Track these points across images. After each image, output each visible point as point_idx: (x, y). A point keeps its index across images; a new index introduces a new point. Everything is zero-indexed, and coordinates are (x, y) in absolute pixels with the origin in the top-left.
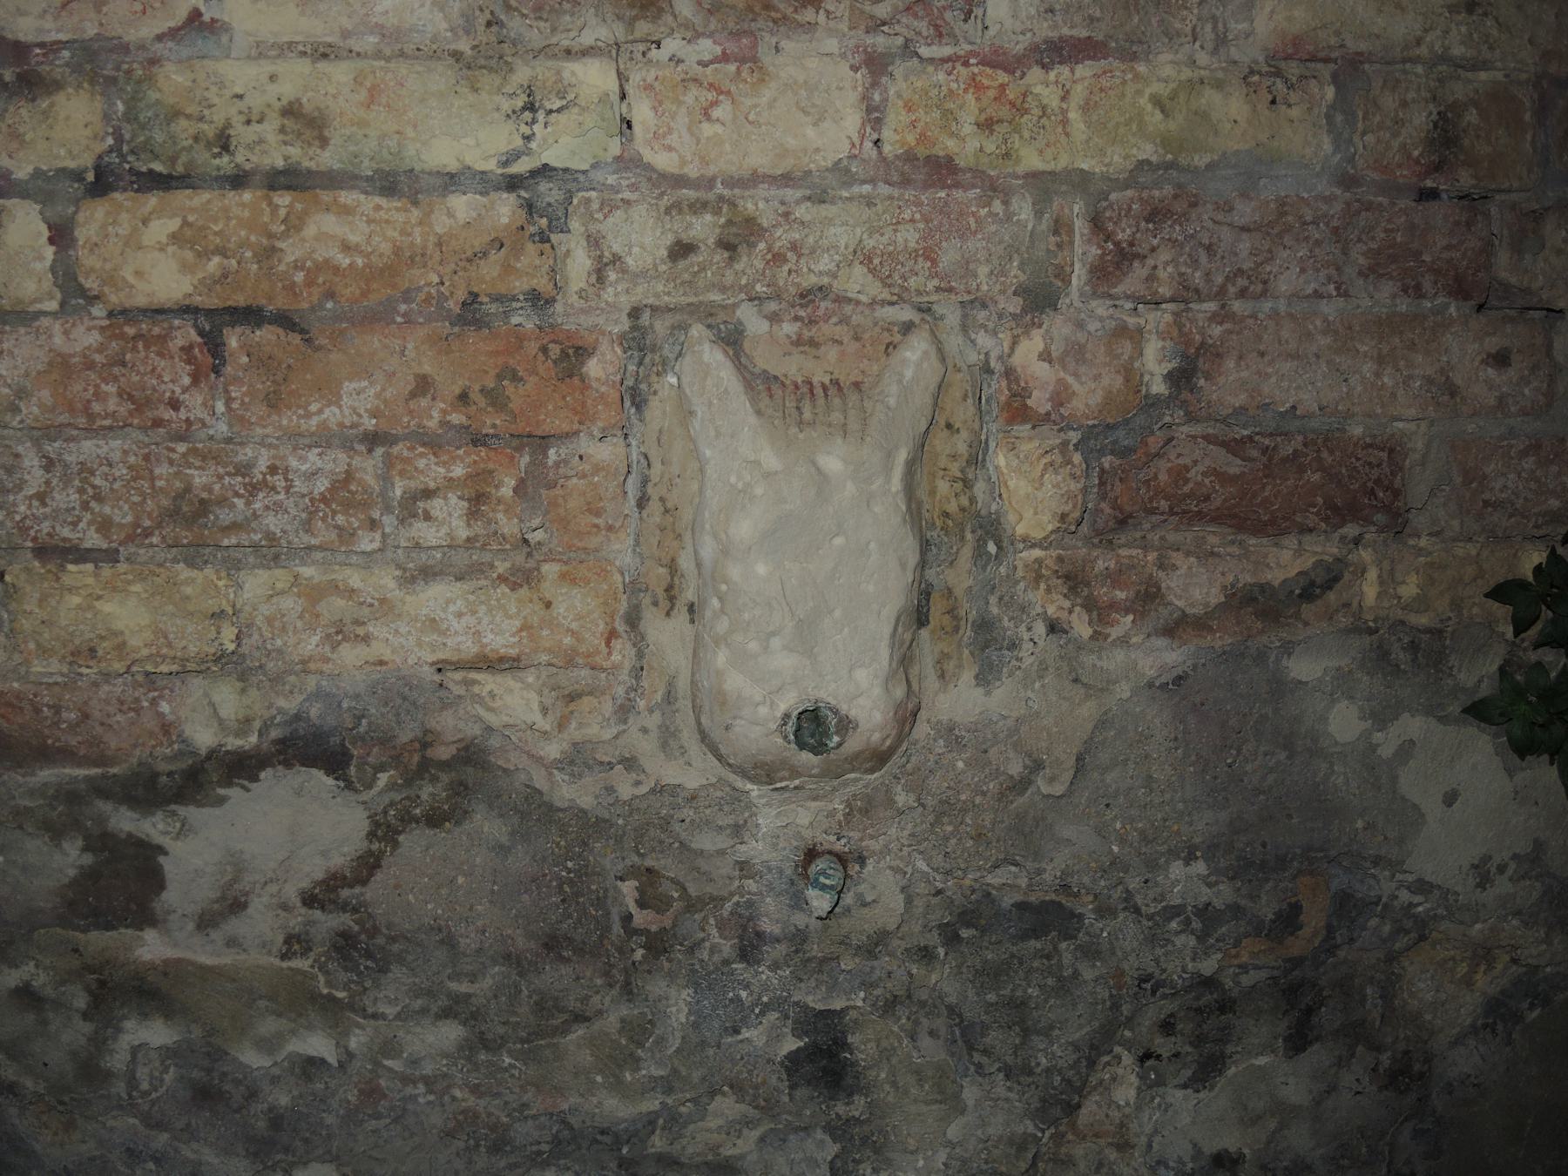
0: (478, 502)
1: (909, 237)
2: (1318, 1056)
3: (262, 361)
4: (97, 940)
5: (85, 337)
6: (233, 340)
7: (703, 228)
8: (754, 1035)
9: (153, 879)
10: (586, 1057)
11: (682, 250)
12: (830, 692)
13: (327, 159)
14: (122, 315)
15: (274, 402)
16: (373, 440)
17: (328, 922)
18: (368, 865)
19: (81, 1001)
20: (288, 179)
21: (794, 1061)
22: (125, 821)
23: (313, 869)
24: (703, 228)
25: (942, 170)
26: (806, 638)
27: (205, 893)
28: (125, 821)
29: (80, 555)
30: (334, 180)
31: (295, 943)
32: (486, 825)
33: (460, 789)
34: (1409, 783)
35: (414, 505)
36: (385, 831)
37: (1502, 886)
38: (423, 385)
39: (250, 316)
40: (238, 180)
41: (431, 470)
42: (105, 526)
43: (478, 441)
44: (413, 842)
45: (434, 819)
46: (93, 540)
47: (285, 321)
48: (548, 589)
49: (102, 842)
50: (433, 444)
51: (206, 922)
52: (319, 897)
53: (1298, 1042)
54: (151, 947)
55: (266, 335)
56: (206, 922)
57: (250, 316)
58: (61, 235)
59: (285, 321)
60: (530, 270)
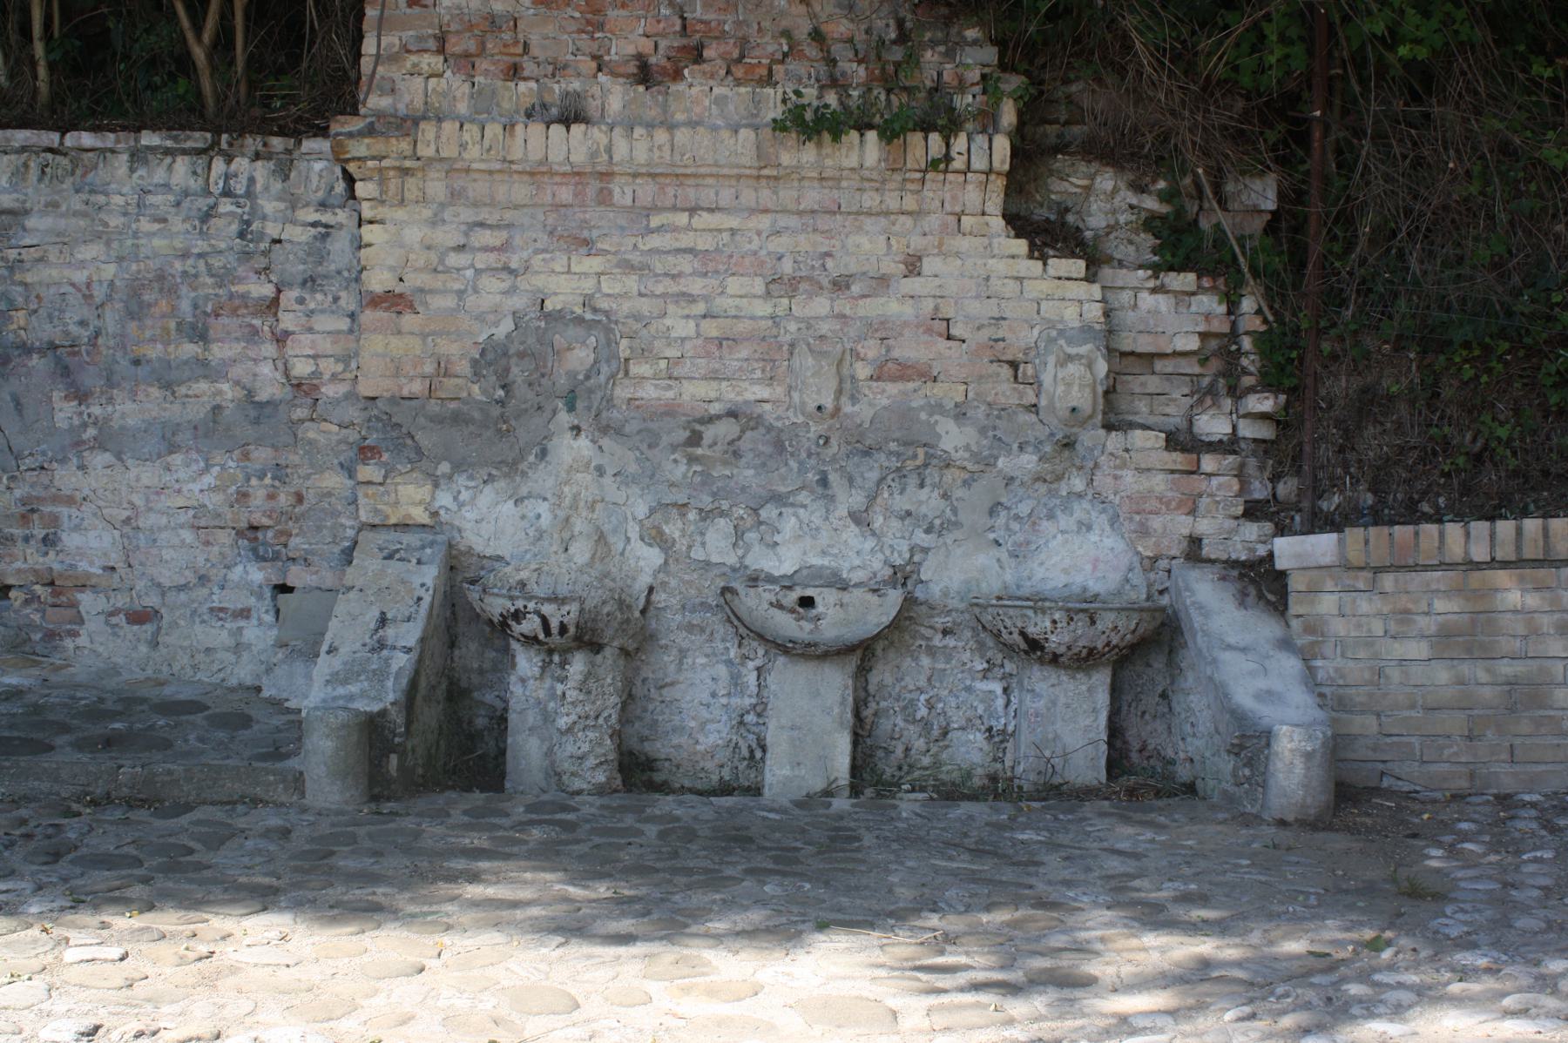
0: (763, 371)
2: (926, 490)
4: (690, 450)
5: (700, 342)
8: (810, 475)
12: (822, 402)
17: (732, 448)
18: (739, 438)
20: (735, 317)
23: (729, 438)
24: (802, 325)
25: (844, 316)
26: (819, 392)
28: (698, 427)
31: (726, 452)
32: (762, 430)
34: (938, 429)
36: (743, 432)
37: (961, 453)
41: (756, 365)
44: (749, 434)
49: (693, 431)
52: (731, 443)
53: (922, 486)
54: (699, 451)
56: (710, 446)
60: (774, 331)
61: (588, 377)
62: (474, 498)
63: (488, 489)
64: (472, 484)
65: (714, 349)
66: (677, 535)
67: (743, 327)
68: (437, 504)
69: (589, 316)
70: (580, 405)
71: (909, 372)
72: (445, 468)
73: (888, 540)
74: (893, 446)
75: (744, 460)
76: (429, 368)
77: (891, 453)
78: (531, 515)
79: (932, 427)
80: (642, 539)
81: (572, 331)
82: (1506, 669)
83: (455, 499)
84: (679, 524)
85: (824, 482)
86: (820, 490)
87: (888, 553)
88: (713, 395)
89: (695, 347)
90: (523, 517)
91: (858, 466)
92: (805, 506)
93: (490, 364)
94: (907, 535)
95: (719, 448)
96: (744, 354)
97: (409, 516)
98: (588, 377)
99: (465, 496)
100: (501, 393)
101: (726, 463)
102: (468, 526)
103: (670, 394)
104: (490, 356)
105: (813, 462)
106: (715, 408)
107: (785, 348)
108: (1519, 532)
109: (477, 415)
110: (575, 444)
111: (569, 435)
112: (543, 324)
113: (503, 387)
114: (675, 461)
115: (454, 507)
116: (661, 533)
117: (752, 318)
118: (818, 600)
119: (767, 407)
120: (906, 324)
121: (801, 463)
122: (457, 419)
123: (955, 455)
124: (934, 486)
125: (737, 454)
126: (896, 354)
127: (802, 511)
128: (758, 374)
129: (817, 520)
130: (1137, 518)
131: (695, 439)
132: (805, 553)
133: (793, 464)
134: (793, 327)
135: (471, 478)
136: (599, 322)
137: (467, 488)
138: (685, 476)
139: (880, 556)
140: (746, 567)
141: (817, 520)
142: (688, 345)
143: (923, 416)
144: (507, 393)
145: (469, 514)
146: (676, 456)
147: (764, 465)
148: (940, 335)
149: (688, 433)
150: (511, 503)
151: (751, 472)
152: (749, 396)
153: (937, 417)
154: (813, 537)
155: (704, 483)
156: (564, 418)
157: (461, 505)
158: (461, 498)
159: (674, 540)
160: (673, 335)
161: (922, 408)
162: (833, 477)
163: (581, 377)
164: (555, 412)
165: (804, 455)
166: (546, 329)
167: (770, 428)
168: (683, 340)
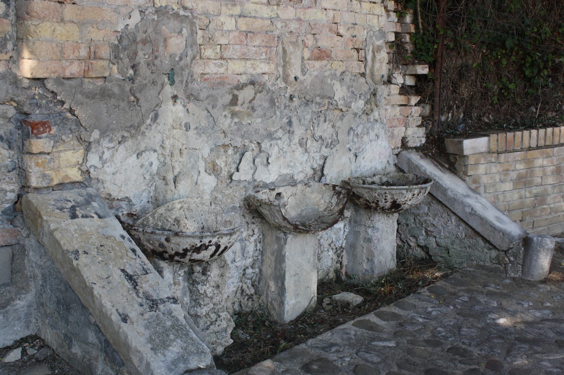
1: (298, 26)
3: (251, 37)
4: (232, 108)
5: (236, 34)
6: (249, 34)
7: (283, 24)
9: (237, 100)
10: (271, 123)
11: (282, 27)
13: (257, 15)
14: (240, 31)
15: (251, 42)
16: (259, 46)
18: (254, 98)
19: (230, 116)
20: (255, 17)
21: (287, 123)
22: (236, 92)
24: (283, 24)
27: (242, 101)
28: (236, 92)
29: (234, 59)
30: (258, 18)
32: (264, 92)
33: (263, 88)
35: (261, 54)
36: (256, 94)
37: (341, 101)
38: (263, 41)
39: (250, 32)
40: (251, 17)
42: (237, 56)
43: (266, 47)
44: (258, 95)
45: (260, 92)
46: (236, 57)
47: (253, 33)
48: (271, 64)
50: (263, 47)
51: (242, 105)
53: (325, 121)
54: (237, 108)
55: (252, 34)
56: (242, 105)
57: (250, 32)
58: (236, 22)
59: (253, 33)
61: (181, 59)
62: (113, 156)
63: (121, 148)
64: (111, 145)
65: (243, 38)
66: (223, 165)
67: (258, 24)
68: (88, 165)
69: (182, 13)
70: (177, 79)
71: (323, 54)
72: (96, 134)
73: (312, 154)
74: (318, 99)
75: (256, 112)
76: (83, 53)
77: (316, 103)
78: (146, 164)
79: (332, 86)
80: (206, 171)
81: (174, 24)
82: (535, 190)
83: (101, 158)
84: (224, 158)
85: (290, 123)
86: (288, 128)
87: (312, 162)
88: (242, 70)
89: (234, 37)
90: (142, 166)
91: (303, 112)
92: (280, 139)
93: (125, 49)
94: (318, 150)
95: (246, 105)
96: (257, 43)
97: (67, 177)
98: (181, 59)
99: (107, 155)
100: (131, 72)
101: (249, 115)
102: (108, 178)
103: (222, 70)
104: (125, 42)
105: (286, 111)
106: (243, 79)
107: (276, 39)
108: (546, 133)
109: (116, 90)
110: (174, 109)
111: (171, 102)
112: (156, 17)
113: (133, 67)
114: (225, 116)
115: (99, 165)
116: (214, 165)
117: (262, 18)
118: (284, 194)
119: (266, 77)
120: (323, 26)
121: (281, 112)
122: (104, 94)
123: (339, 103)
124: (330, 121)
125: (253, 109)
126: (319, 44)
127: (279, 141)
128: (264, 56)
129: (286, 148)
130: (391, 129)
131: (234, 101)
132: (280, 168)
133: (278, 113)
134: (279, 25)
135: (111, 141)
136: (187, 17)
137: (108, 148)
138: (230, 126)
139: (309, 164)
140: (255, 181)
141: (286, 148)
142: (231, 36)
143: (329, 81)
144: (135, 72)
145: (109, 169)
146: (225, 113)
147: (265, 115)
148: (335, 33)
149: (230, 97)
150: (135, 156)
151: (259, 120)
152: (259, 71)
153: (334, 81)
154: (284, 157)
155: (238, 130)
156: (169, 90)
157: (104, 163)
158: (105, 157)
159: (221, 169)
160: (225, 28)
161: (328, 77)
162: (294, 120)
163: (177, 59)
164: (163, 86)
165: (283, 107)
166: (158, 21)
167: (269, 91)
168: (230, 31)
